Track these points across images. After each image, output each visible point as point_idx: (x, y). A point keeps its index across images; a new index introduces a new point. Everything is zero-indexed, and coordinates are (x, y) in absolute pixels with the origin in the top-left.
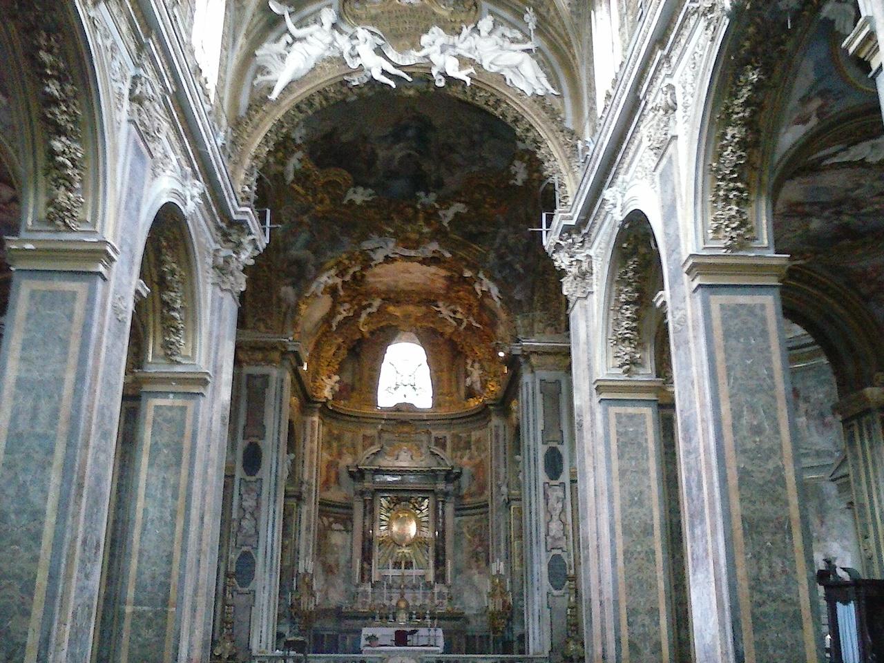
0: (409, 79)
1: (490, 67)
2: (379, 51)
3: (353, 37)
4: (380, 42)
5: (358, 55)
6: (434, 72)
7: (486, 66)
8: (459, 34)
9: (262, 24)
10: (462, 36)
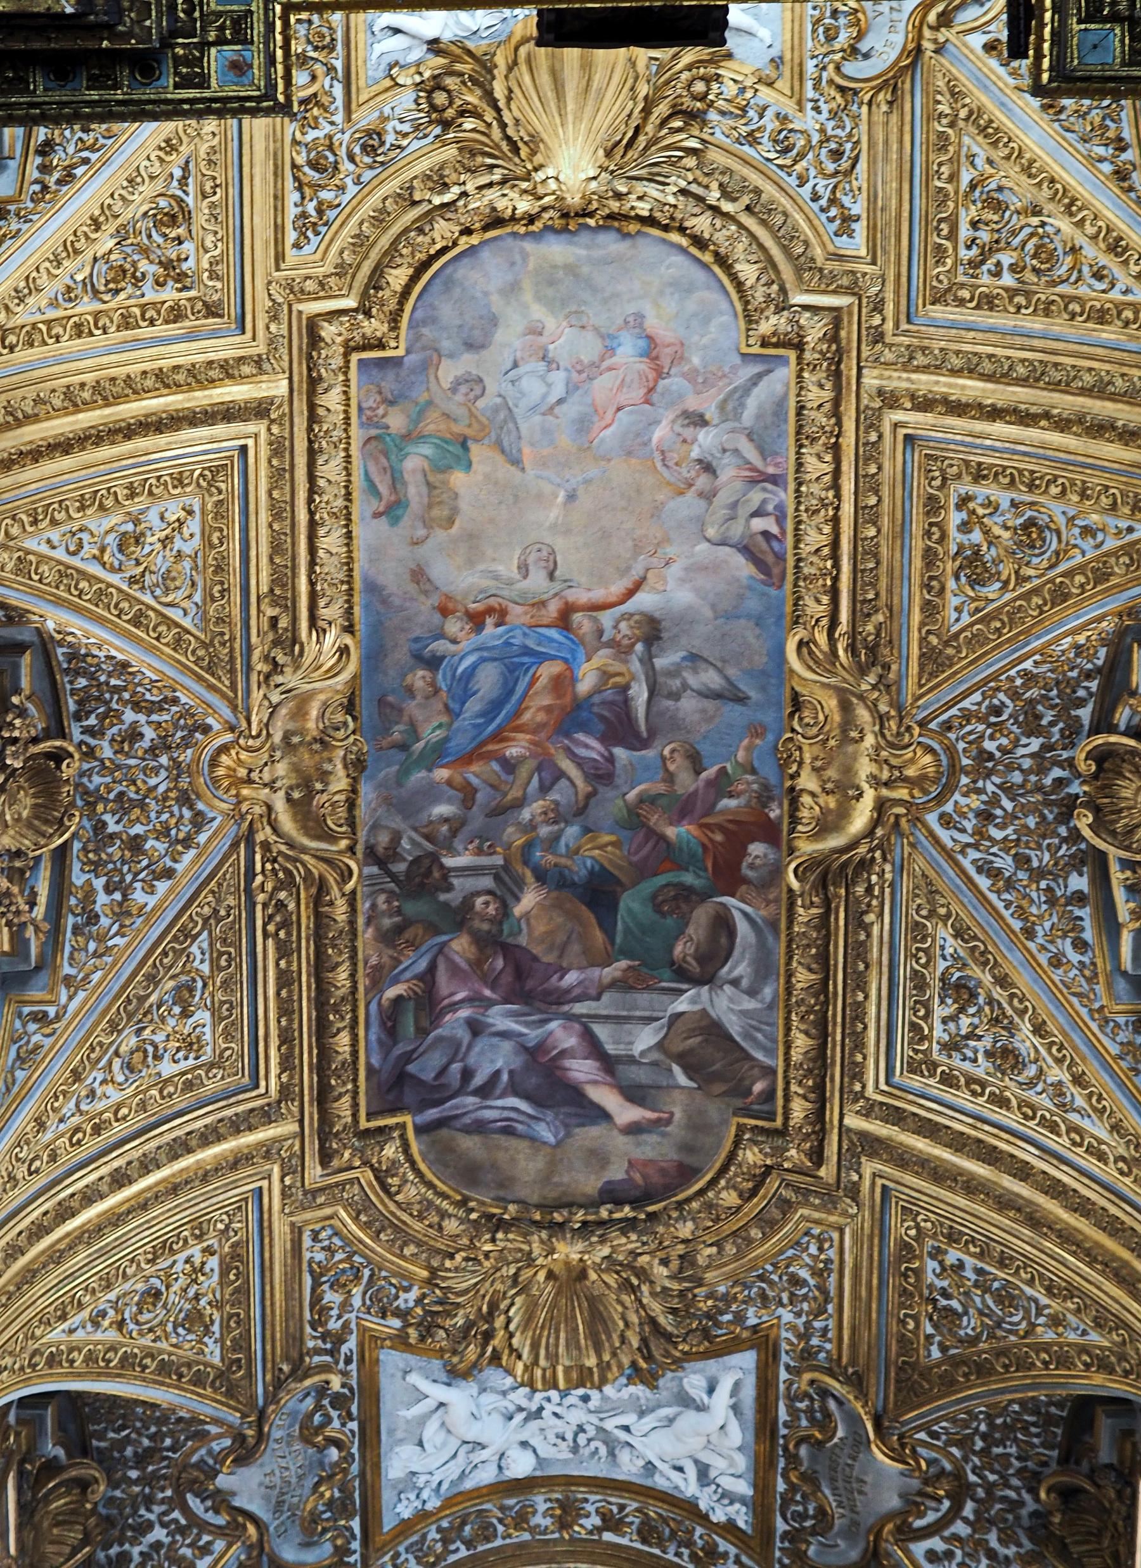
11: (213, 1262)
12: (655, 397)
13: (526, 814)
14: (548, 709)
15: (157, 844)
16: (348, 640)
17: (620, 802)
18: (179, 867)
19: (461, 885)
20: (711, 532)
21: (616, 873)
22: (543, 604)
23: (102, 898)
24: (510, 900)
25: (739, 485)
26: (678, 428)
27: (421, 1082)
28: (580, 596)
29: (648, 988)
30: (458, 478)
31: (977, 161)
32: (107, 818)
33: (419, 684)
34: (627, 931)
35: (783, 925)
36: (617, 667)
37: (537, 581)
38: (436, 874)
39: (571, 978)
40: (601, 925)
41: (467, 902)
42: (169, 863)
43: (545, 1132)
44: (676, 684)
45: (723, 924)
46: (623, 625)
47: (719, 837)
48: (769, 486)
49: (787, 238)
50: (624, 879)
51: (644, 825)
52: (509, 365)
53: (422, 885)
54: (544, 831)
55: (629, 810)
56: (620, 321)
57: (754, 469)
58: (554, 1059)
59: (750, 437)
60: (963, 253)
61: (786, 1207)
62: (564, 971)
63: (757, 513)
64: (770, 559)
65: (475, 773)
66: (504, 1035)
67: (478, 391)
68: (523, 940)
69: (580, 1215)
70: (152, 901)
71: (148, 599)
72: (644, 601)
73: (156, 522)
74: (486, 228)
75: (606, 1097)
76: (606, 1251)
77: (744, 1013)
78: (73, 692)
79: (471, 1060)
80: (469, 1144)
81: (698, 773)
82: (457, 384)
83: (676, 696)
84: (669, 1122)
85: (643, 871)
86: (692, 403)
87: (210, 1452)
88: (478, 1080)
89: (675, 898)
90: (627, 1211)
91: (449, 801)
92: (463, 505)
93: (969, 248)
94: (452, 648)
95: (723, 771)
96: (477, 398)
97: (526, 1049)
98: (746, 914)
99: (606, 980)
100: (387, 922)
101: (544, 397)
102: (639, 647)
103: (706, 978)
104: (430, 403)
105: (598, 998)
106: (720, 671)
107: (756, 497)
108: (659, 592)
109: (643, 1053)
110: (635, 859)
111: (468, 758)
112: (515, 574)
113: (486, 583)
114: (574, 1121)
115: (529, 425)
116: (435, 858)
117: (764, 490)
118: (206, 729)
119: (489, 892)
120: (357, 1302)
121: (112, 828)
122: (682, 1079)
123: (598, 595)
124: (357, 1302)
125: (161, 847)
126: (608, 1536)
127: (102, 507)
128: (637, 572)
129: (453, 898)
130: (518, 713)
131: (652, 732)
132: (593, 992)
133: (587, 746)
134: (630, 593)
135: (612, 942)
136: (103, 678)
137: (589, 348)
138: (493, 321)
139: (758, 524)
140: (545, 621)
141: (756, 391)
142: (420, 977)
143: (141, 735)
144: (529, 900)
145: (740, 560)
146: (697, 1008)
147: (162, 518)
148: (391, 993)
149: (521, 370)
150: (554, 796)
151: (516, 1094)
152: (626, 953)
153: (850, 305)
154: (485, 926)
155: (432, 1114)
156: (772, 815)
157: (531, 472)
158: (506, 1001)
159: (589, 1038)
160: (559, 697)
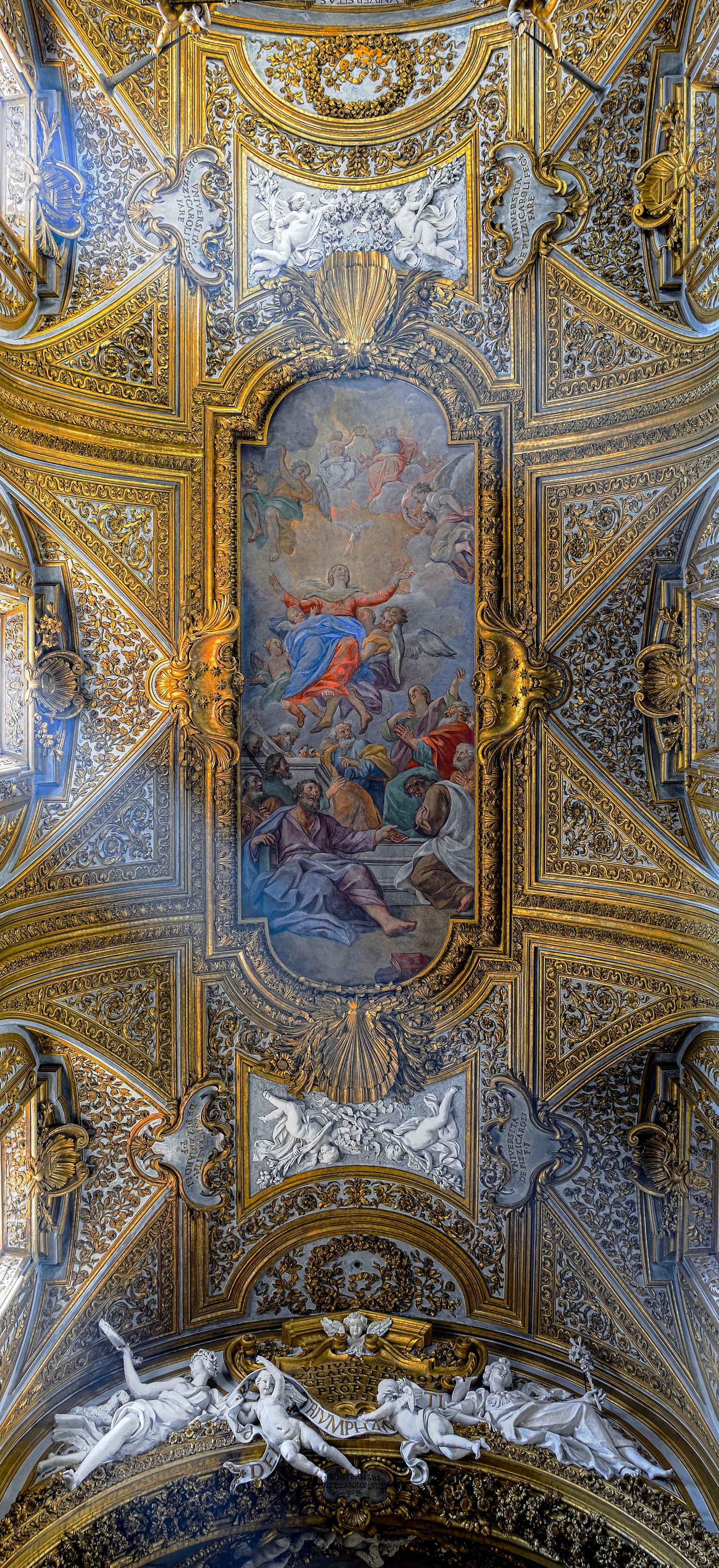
0: (356, 1472)
1: (517, 1435)
2: (295, 1411)
3: (250, 1388)
4: (299, 1399)
5: (257, 1422)
6: (406, 1452)
7: (508, 1433)
8: (450, 1392)
9: (76, 1375)
10: (456, 1395)
11: (154, 994)
12: (402, 476)
13: (333, 732)
14: (345, 666)
15: (125, 726)
16: (234, 609)
17: (385, 724)
18: (138, 738)
19: (297, 776)
20: (434, 555)
21: (383, 770)
22: (342, 601)
23: (94, 753)
24: (324, 786)
25: (448, 525)
26: (415, 494)
27: (273, 900)
28: (363, 597)
29: (402, 842)
30: (296, 523)
31: (570, 311)
32: (98, 709)
33: (273, 647)
34: (390, 806)
35: (477, 793)
36: (383, 640)
37: (339, 586)
38: (282, 767)
39: (359, 836)
40: (375, 803)
41: (299, 789)
42: (132, 736)
43: (345, 939)
44: (416, 649)
45: (444, 798)
46: (386, 614)
47: (441, 743)
48: (465, 523)
49: (472, 373)
50: (388, 774)
51: (399, 738)
52: (323, 457)
53: (274, 773)
54: (343, 743)
55: (391, 730)
56: (383, 432)
57: (457, 515)
58: (349, 889)
59: (454, 496)
60: (565, 366)
61: (481, 973)
62: (355, 832)
63: (458, 541)
64: (466, 567)
65: (304, 705)
66: (319, 872)
67: (306, 472)
68: (331, 812)
69: (364, 989)
70: (122, 755)
71: (123, 560)
72: (398, 598)
73: (130, 517)
74: (311, 374)
75: (378, 913)
76: (379, 1008)
77: (455, 853)
78: (82, 625)
79: (302, 888)
80: (301, 942)
81: (428, 704)
82: (296, 466)
83: (415, 656)
84: (414, 928)
85: (398, 769)
86: (422, 479)
87: (150, 1128)
88: (305, 902)
89: (416, 784)
90: (391, 986)
91: (290, 721)
92: (298, 541)
93: (567, 362)
94: (292, 626)
95: (442, 701)
96: (306, 476)
97: (333, 882)
98: (456, 790)
99: (378, 839)
100: (255, 794)
101: (343, 477)
102: (395, 627)
103: (435, 835)
104: (280, 477)
105: (374, 850)
106: (440, 639)
107: (458, 531)
108: (405, 593)
109: (399, 884)
110: (394, 760)
111: (301, 696)
112: (326, 583)
113: (311, 588)
114: (361, 929)
115: (334, 494)
116: (281, 756)
117: (463, 526)
118: (154, 658)
119: (313, 781)
120: (236, 1040)
121: (100, 716)
122: (422, 900)
123: (372, 596)
124: (236, 1040)
125: (128, 727)
126: (381, 1206)
127: (99, 495)
128: (394, 581)
129: (292, 783)
130: (328, 669)
131: (403, 680)
132: (371, 846)
133: (366, 690)
134: (391, 595)
135: (382, 814)
136: (98, 616)
137: (366, 448)
138: (315, 431)
139: (459, 547)
140: (344, 612)
141: (457, 468)
142: (273, 832)
143: (118, 661)
144: (335, 786)
145: (450, 569)
146: (430, 853)
147: (133, 516)
148: (256, 840)
149: (331, 460)
150: (348, 721)
151: (327, 911)
152: (389, 820)
153: (506, 408)
154: (310, 803)
155: (279, 922)
156: (470, 725)
157: (335, 522)
158: (322, 851)
159: (368, 873)
160: (351, 659)
